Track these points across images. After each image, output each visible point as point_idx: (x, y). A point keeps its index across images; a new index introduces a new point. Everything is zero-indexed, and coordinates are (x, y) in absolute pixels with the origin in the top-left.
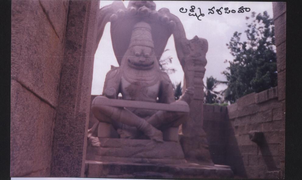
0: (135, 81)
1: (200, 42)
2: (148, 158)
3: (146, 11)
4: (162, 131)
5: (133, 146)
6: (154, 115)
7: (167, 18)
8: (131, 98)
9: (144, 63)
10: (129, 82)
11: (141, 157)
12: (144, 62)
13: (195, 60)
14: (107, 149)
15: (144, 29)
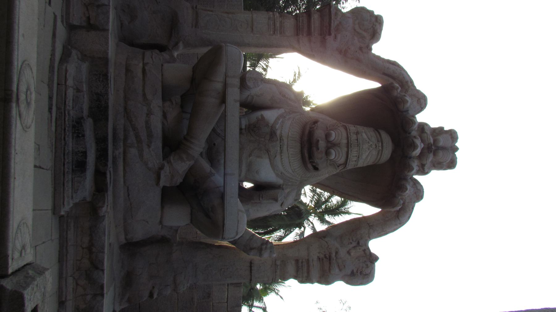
0: (278, 133)
1: (367, 266)
2: (125, 152)
3: (413, 146)
4: (181, 183)
5: (147, 123)
6: (213, 171)
7: (407, 189)
8: (243, 127)
9: (315, 149)
10: (276, 121)
11: (126, 138)
12: (318, 149)
13: (330, 259)
14: (140, 75)
15: (380, 148)
